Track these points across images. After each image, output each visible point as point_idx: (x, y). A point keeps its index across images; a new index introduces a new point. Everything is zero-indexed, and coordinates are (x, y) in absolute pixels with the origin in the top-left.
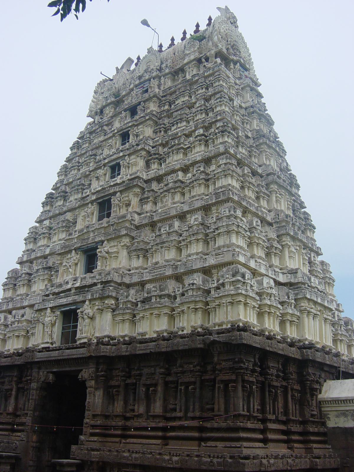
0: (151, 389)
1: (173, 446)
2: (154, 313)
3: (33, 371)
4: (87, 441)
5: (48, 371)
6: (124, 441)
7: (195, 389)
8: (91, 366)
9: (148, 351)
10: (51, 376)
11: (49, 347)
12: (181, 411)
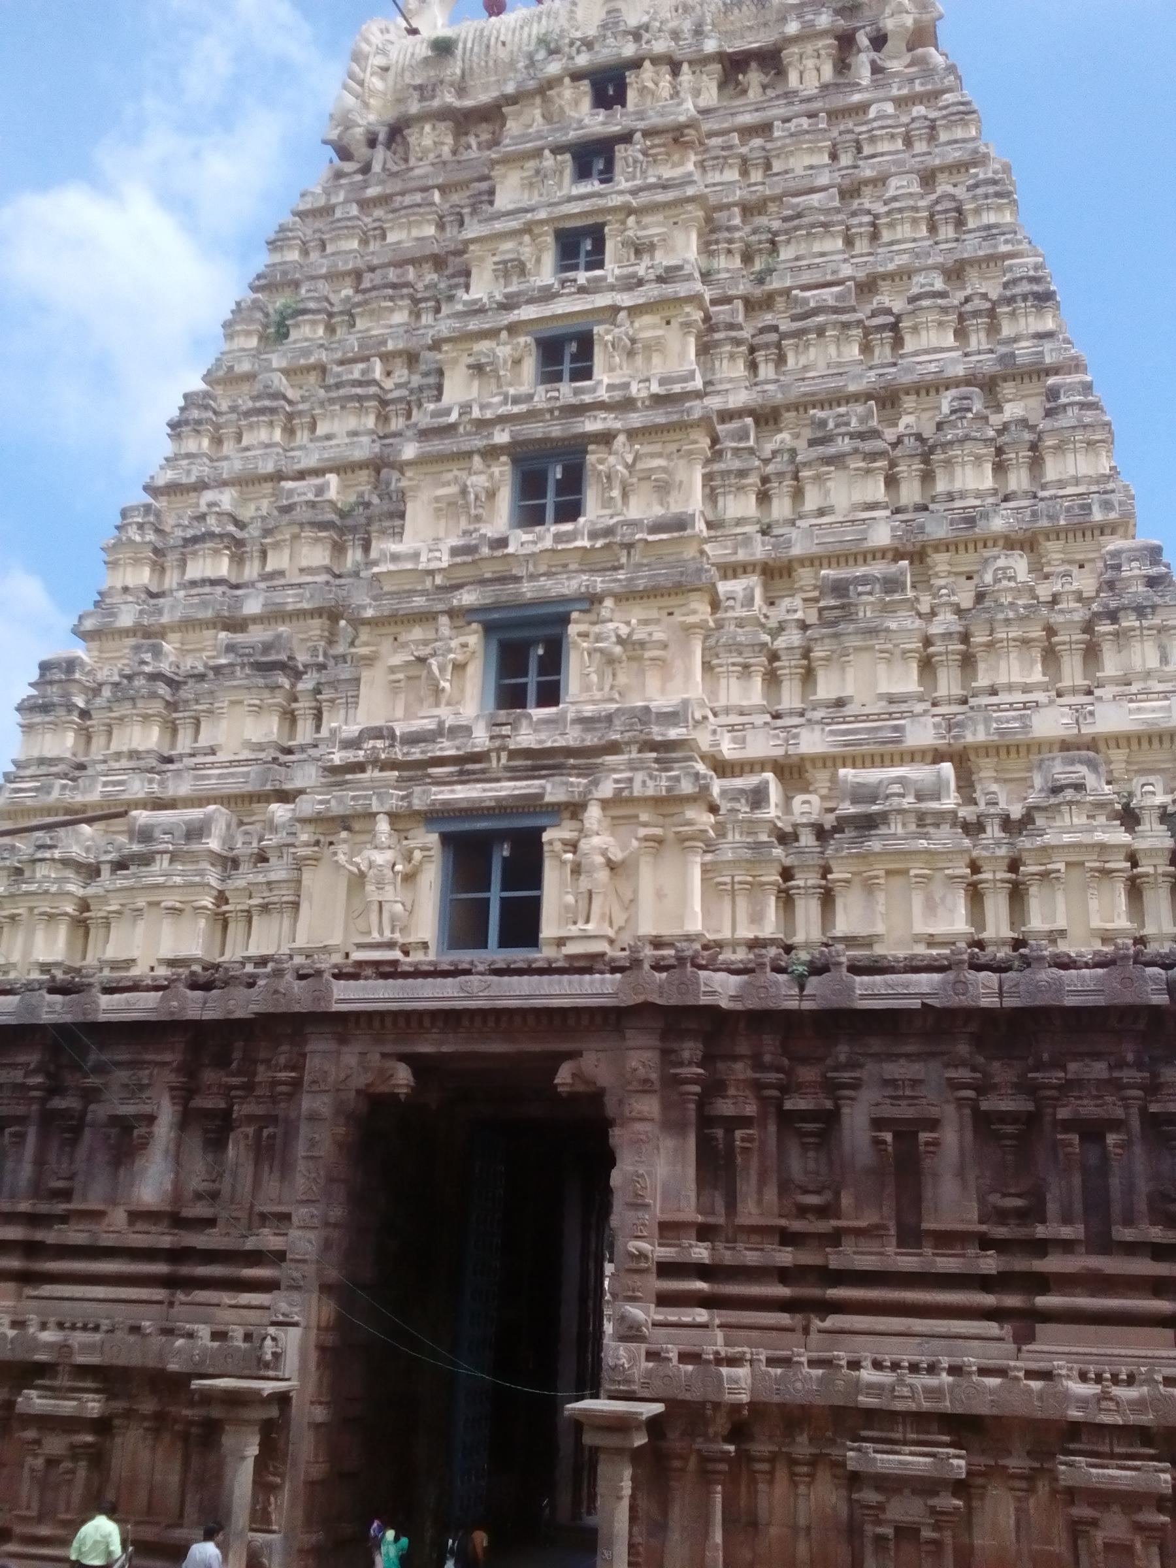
0: (739, 1134)
2: (912, 872)
3: (309, 1048)
4: (655, 1324)
5: (388, 1048)
6: (817, 1323)
7: (1126, 1145)
8: (630, 1043)
9: (916, 1004)
10: (403, 1076)
11: (395, 963)
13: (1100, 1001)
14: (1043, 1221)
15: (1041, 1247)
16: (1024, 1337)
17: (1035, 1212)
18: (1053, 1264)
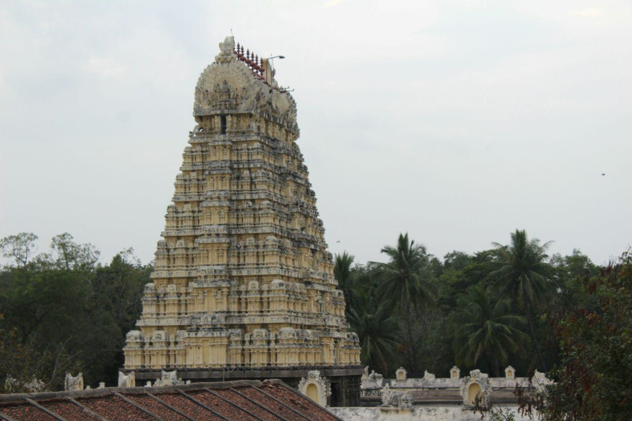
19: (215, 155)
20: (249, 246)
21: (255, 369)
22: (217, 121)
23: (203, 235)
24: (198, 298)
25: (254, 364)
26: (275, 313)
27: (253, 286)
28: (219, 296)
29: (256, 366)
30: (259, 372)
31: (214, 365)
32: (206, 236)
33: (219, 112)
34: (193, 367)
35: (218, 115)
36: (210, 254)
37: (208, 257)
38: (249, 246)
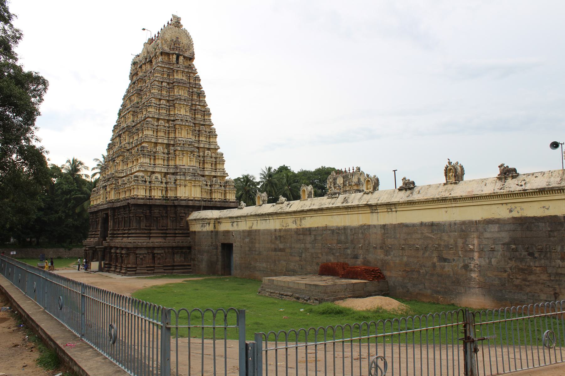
1: (152, 240)
12: (154, 227)
13: (159, 204)
14: (151, 227)
15: (151, 230)
16: (150, 239)
17: (150, 226)
18: (152, 231)
19: (178, 75)
20: (202, 131)
21: (216, 201)
22: (175, 56)
23: (179, 119)
24: (180, 156)
25: (215, 199)
26: (220, 170)
27: (208, 153)
28: (192, 157)
29: (216, 200)
30: (219, 203)
31: (195, 197)
32: (180, 120)
33: (177, 52)
34: (181, 198)
35: (175, 54)
36: (183, 131)
37: (181, 133)
38: (202, 131)
